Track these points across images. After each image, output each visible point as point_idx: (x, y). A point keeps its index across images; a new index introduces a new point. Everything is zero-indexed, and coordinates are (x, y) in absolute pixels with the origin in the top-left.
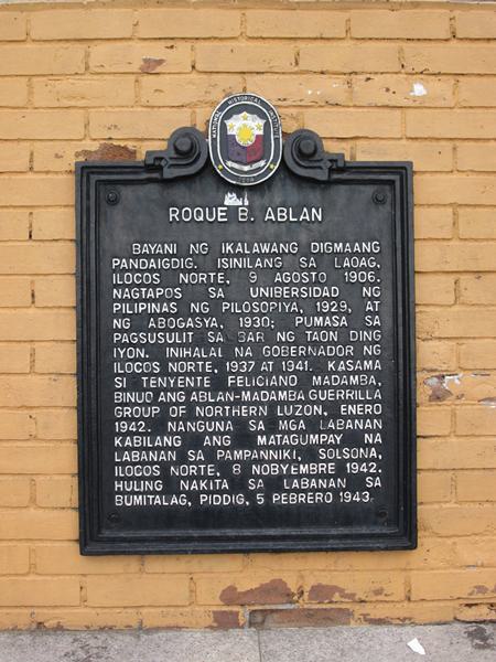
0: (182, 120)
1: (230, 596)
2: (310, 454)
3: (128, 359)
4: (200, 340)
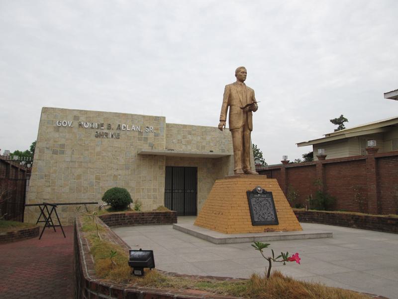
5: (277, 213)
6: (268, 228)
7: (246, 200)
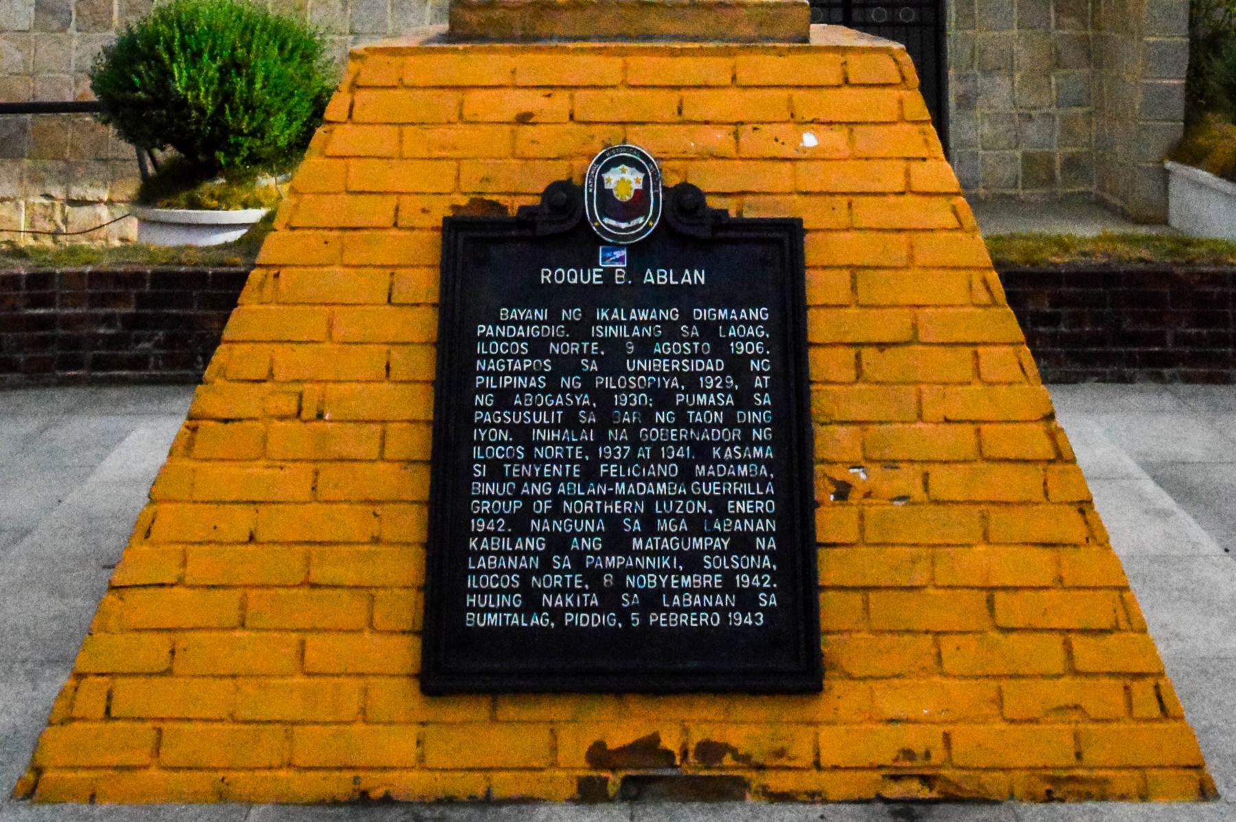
0: (559, 172)
1: (599, 755)
2: (692, 562)
3: (492, 437)
4: (570, 419)
5: (832, 521)
6: (648, 748)
7: (421, 324)
